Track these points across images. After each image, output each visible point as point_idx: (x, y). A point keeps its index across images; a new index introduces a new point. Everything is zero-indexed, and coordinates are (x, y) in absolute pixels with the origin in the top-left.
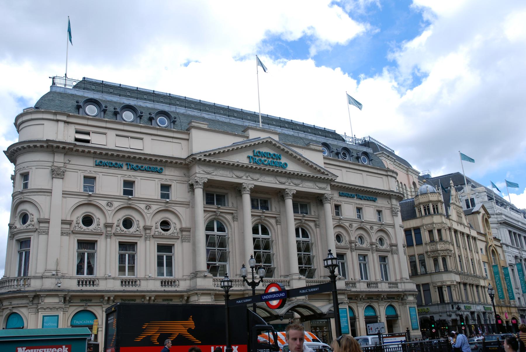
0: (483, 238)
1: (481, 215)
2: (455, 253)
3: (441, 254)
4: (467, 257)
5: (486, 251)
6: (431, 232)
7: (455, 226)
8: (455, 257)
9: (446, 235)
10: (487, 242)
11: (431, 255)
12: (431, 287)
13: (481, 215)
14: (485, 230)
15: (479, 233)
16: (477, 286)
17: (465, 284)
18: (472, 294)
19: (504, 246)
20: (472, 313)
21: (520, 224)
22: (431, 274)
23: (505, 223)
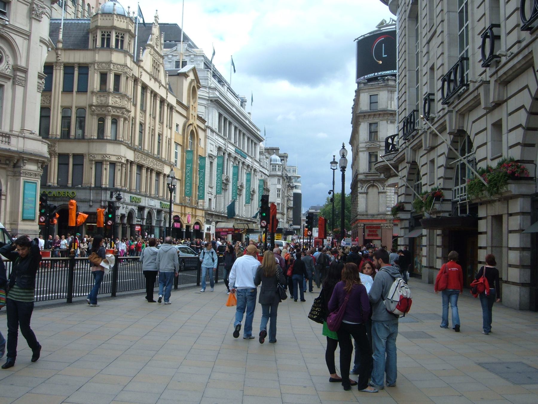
0: (184, 113)
1: (189, 80)
2: (134, 119)
3: (112, 113)
4: (154, 130)
5: (184, 130)
6: (104, 77)
7: (145, 78)
8: (134, 124)
9: (127, 87)
10: (187, 118)
11: (97, 112)
12: (86, 161)
13: (189, 80)
14: (189, 101)
15: (179, 103)
16: (158, 174)
17: (140, 167)
18: (149, 183)
19: (208, 131)
20: (141, 209)
21: (234, 110)
22: (91, 140)
23: (217, 103)
